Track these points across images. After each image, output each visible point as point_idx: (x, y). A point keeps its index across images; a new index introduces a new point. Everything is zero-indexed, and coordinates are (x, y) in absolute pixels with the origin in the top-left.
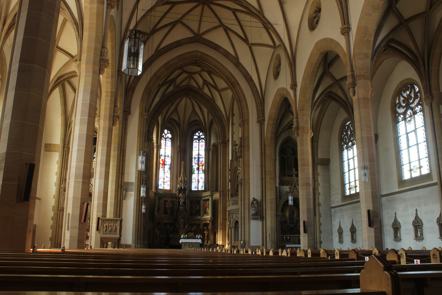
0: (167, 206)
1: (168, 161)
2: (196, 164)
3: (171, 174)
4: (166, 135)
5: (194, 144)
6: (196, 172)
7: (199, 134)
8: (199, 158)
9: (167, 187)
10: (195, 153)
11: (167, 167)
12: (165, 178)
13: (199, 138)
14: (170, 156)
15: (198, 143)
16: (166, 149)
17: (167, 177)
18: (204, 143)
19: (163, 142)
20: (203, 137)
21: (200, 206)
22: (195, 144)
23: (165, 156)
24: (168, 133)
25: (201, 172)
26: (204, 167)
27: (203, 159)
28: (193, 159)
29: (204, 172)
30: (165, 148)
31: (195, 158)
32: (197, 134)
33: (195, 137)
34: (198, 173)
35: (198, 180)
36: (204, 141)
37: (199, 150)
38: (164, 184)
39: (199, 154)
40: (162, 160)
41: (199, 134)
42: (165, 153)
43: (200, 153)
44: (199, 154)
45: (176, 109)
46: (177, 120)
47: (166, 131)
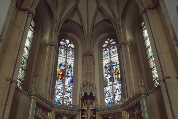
1: (70, 72)
2: (108, 74)
4: (67, 45)
5: (103, 52)
10: (106, 62)
11: (68, 80)
12: (66, 93)
13: (109, 45)
14: (73, 67)
15: (108, 51)
16: (66, 59)
17: (68, 92)
18: (116, 49)
20: (114, 43)
25: (116, 81)
26: (119, 75)
29: (121, 81)
31: (106, 67)
32: (107, 42)
33: (104, 46)
38: (63, 101)
39: (111, 62)
40: (62, 71)
41: (109, 41)
44: (111, 62)
45: (76, 9)
46: (78, 21)
47: (68, 41)
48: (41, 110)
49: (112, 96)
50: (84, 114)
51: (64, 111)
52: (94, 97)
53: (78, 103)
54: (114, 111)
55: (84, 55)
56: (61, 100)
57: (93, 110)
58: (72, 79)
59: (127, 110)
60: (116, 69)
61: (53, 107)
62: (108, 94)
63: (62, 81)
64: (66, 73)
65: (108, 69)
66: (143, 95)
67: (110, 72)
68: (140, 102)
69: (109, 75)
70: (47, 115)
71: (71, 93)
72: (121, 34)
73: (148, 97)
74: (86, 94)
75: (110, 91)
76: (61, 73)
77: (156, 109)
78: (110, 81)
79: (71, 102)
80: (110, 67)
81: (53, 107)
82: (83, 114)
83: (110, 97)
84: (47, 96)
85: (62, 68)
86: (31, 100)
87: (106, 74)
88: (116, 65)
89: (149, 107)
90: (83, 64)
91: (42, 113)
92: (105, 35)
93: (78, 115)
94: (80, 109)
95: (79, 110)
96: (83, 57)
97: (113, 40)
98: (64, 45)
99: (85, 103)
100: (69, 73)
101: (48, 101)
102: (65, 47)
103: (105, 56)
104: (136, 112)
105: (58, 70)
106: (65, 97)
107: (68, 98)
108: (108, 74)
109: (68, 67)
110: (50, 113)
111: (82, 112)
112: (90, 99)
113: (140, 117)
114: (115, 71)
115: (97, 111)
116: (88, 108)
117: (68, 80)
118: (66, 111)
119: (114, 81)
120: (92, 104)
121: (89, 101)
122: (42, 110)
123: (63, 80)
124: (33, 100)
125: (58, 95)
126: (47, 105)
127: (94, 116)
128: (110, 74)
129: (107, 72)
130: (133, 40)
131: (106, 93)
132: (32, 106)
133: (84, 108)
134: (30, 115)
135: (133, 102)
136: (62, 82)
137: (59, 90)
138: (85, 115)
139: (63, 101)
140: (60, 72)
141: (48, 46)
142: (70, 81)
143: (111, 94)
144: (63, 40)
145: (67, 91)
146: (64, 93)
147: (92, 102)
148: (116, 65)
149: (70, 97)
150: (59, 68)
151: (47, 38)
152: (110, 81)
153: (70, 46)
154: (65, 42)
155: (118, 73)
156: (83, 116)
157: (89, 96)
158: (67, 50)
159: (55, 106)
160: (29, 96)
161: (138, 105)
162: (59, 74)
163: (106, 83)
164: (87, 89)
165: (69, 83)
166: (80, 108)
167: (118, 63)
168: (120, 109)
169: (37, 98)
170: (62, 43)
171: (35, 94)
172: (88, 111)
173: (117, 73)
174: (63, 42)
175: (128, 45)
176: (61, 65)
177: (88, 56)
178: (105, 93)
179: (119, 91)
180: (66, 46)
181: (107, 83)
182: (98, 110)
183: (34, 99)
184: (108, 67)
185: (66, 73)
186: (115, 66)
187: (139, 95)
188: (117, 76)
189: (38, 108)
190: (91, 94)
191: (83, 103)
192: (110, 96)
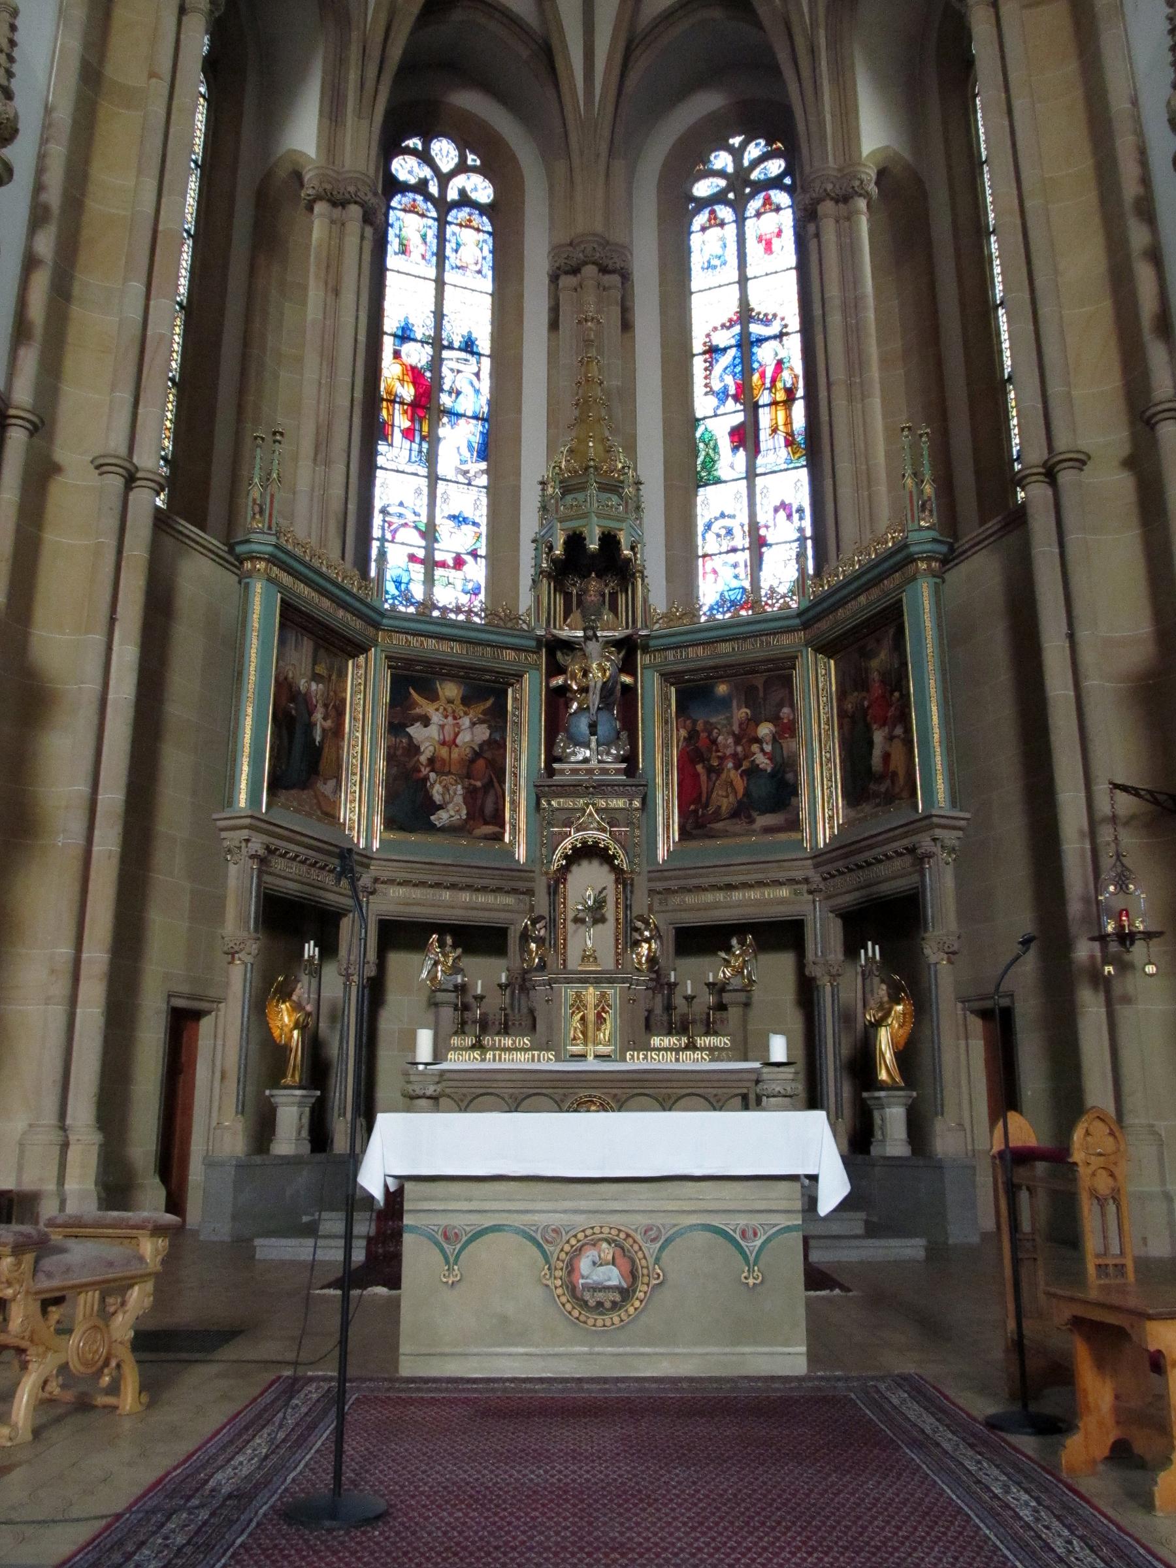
0: (426, 737)
1: (469, 386)
2: (723, 396)
3: (492, 490)
4: (444, 179)
5: (696, 240)
6: (730, 463)
7: (737, 154)
8: (747, 344)
9: (459, 591)
10: (710, 312)
11: (458, 440)
12: (444, 527)
13: (741, 189)
14: (484, 345)
15: (731, 230)
16: (439, 285)
17: (459, 520)
18: (786, 219)
19: (409, 225)
20: (775, 167)
21: (788, 729)
22: (708, 243)
23: (437, 343)
24: (462, 168)
25: (773, 452)
26: (799, 409)
27: (792, 349)
28: (699, 364)
29: (814, 448)
30: (440, 283)
31: (713, 351)
32: (722, 160)
33: (703, 188)
34: (751, 475)
35: (754, 526)
36: (781, 198)
37: (743, 281)
38: (429, 581)
39: (745, 314)
40: (415, 375)
41: (737, 154)
42: (439, 315)
43: (759, 302)
44: (745, 314)
47: (445, 152)
48: (307, 645)
49: (743, 550)
50: (561, 670)
51: (444, 647)
52: (628, 561)
53: (525, 601)
54: (752, 651)
55: (565, 269)
56: (418, 571)
57: (618, 644)
58: (486, 436)
59: (826, 648)
60: (779, 365)
61: (377, 626)
62: (718, 536)
63: (415, 446)
64: (442, 390)
65: (725, 360)
66: (922, 559)
67: (738, 386)
68: (901, 600)
69: (731, 404)
70: (342, 674)
71: (475, 524)
72: (820, 113)
73: (959, 574)
74: (575, 541)
75: (733, 517)
76: (407, 392)
77: (995, 642)
78: (735, 449)
79: (476, 592)
80: (739, 346)
81: (377, 626)
82: (555, 669)
83: (732, 558)
84: (333, 560)
85: (417, 354)
86: (247, 584)
87: (713, 401)
88: (780, 336)
89: (954, 636)
90: (554, 325)
91: (315, 663)
92: (708, 102)
93: (527, 676)
94: (539, 640)
95: (533, 643)
96: (554, 278)
97: (769, 143)
98: (424, 183)
99: (567, 596)
100: (458, 393)
101: (349, 593)
102: (428, 197)
103: (709, 266)
104: (875, 663)
105: (390, 370)
106: (438, 556)
107: (459, 563)
108: (723, 401)
109: (450, 347)
110: (362, 658)
111: (551, 655)
112: (599, 576)
113: (897, 694)
114: (774, 381)
115: (646, 649)
116: (590, 633)
117: (458, 440)
118: (457, 647)
119: (763, 446)
120: (614, 608)
121: (594, 585)
122: (311, 643)
123: (423, 438)
124: (258, 587)
125: (392, 541)
126: (341, 613)
127: (627, 679)
128: (736, 398)
129: (717, 386)
130: (907, 155)
131: (708, 526)
132: (256, 625)
133: (565, 633)
134: (252, 678)
135: (862, 599)
136: (420, 452)
137: (401, 510)
138: (574, 677)
139: (429, 581)
140: (402, 381)
141: (320, 207)
142: (470, 446)
143: (738, 532)
144: (415, 142)
145: (453, 517)
146: (436, 529)
147: (613, 596)
148: (780, 336)
149: (474, 554)
150: (397, 355)
151: (304, 135)
152: (735, 449)
153: (462, 192)
154: (425, 157)
155: (790, 392)
156: (559, 681)
157: (593, 556)
158: (442, 223)
159: (385, 621)
160: (234, 559)
161: (889, 621)
162: (393, 402)
163: (710, 463)
164: (586, 515)
165: (463, 462)
166: (539, 633)
167: (794, 324)
168: (786, 640)
169: (286, 579)
170: (405, 168)
171: (270, 549)
172: (593, 647)
173: (781, 396)
174: (412, 161)
175: (862, 204)
176: (404, 335)
177: (590, 271)
178: (700, 529)
179: (789, 517)
180: (433, 189)
181: (714, 461)
182: (652, 643)
183: (270, 580)
184: (725, 350)
185: (442, 390)
186: (773, 344)
187: (899, 561)
188: (781, 415)
189: (291, 638)
190: (609, 541)
191: (560, 600)
192: (734, 550)
